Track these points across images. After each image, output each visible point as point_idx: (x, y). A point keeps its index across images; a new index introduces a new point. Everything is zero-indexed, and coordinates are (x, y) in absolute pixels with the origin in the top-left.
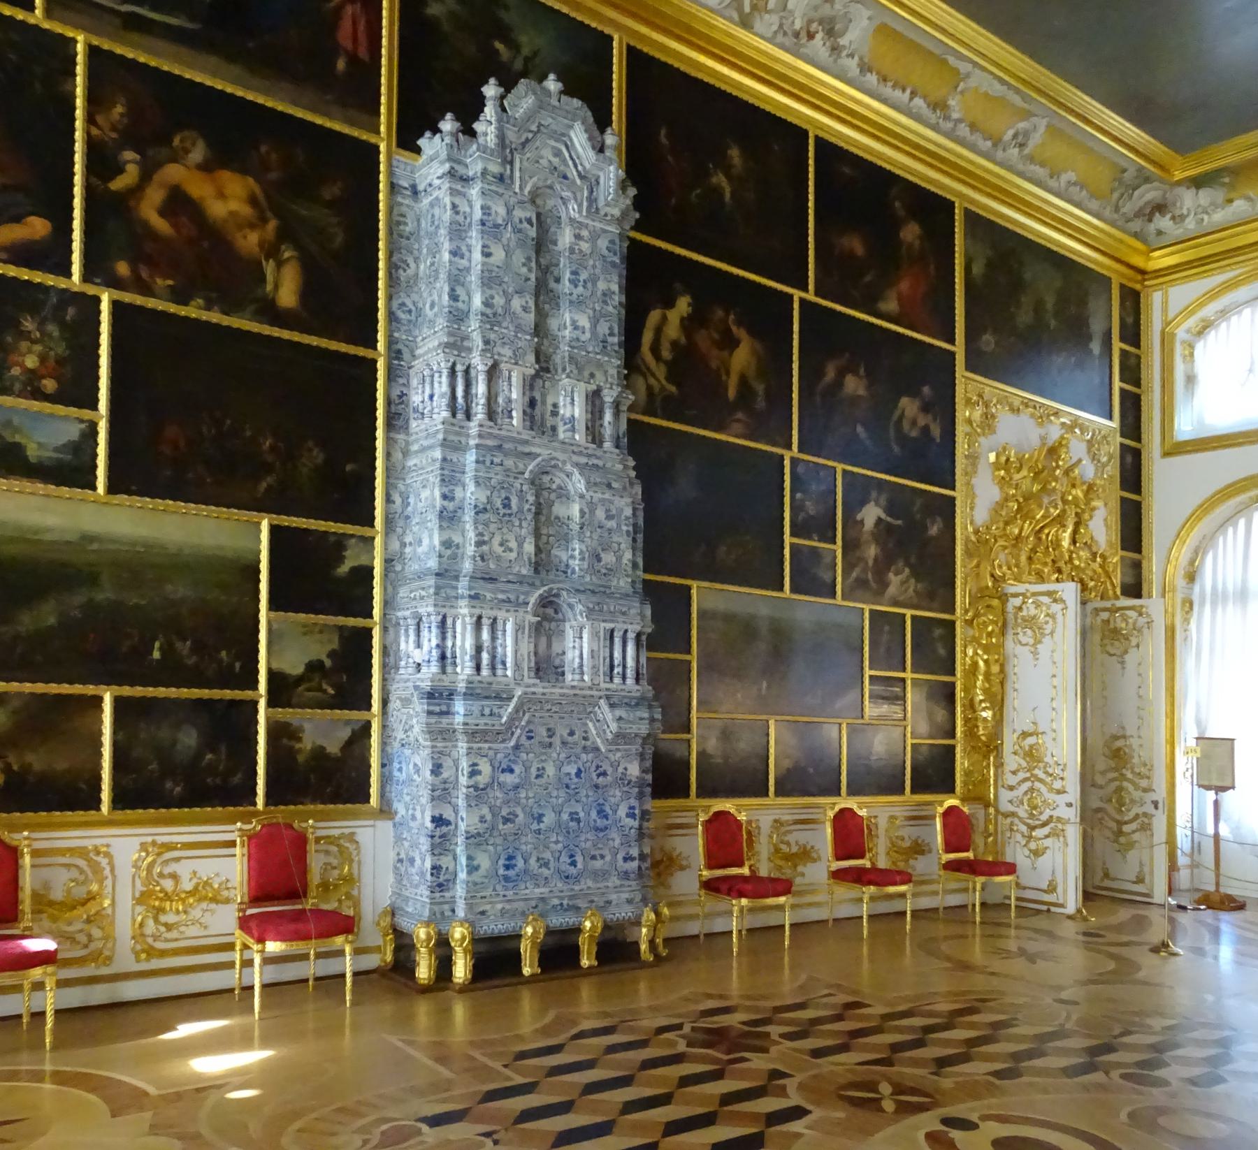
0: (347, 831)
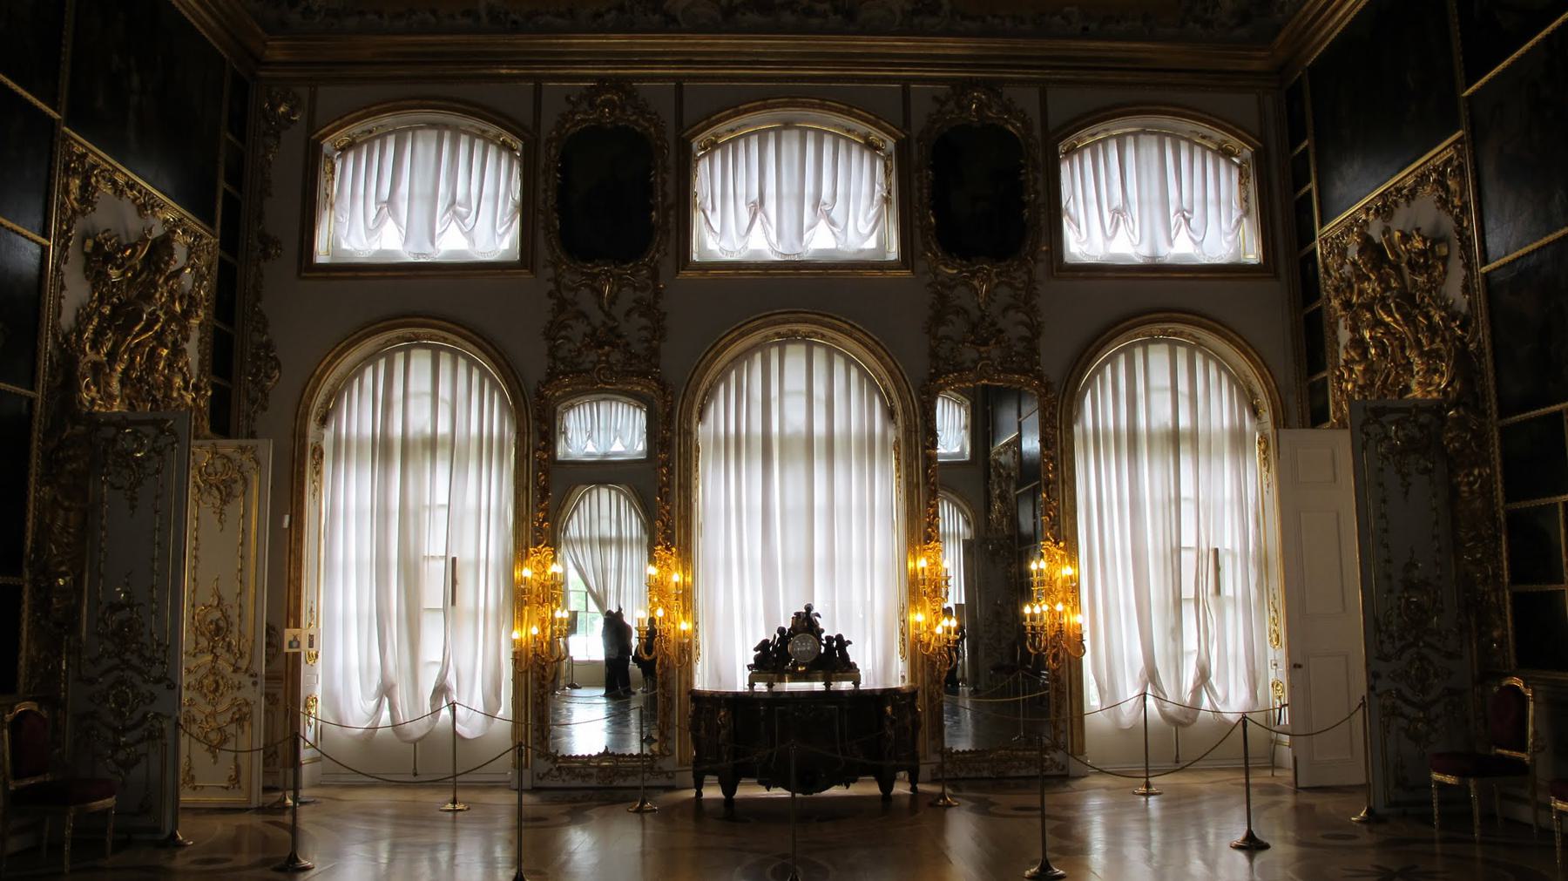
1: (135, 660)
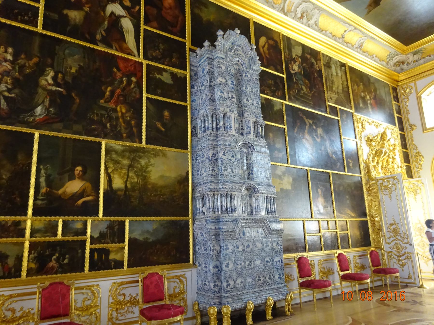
0: (183, 273)
1: (399, 238)
